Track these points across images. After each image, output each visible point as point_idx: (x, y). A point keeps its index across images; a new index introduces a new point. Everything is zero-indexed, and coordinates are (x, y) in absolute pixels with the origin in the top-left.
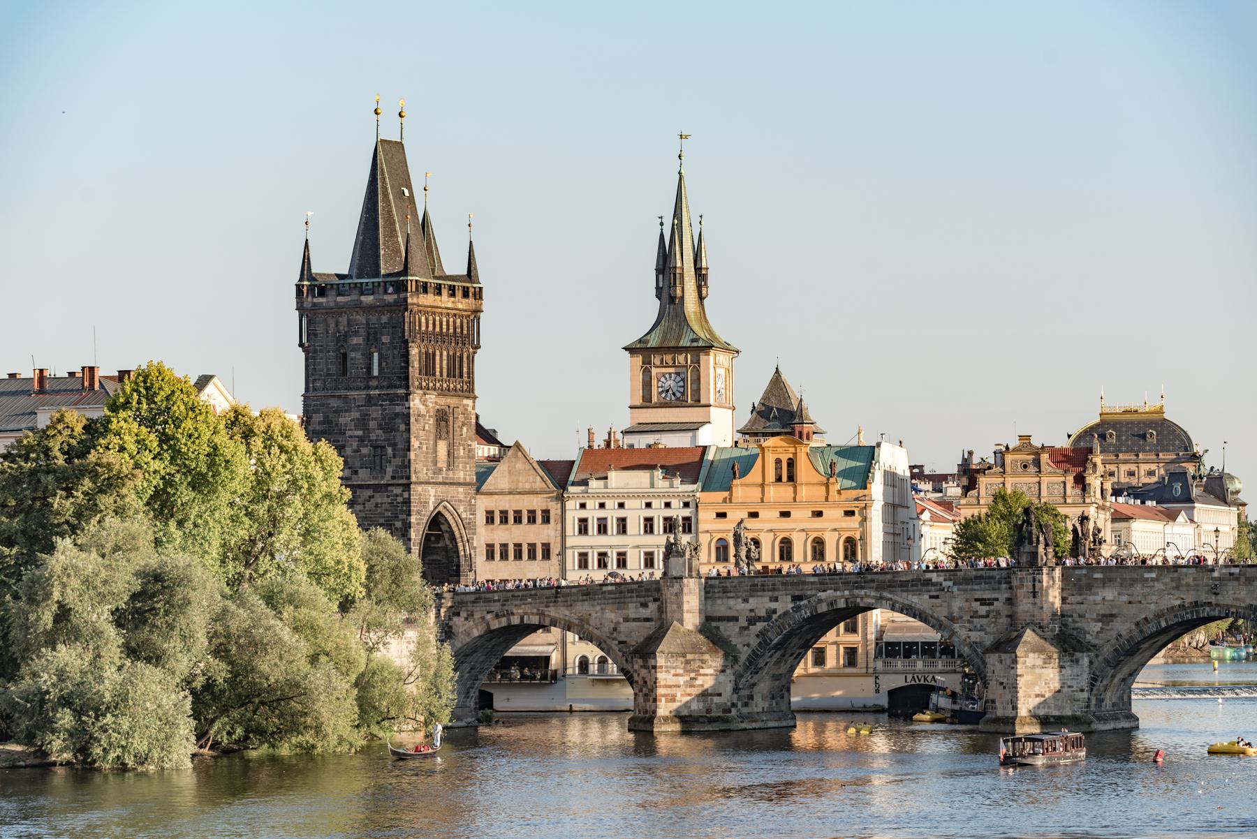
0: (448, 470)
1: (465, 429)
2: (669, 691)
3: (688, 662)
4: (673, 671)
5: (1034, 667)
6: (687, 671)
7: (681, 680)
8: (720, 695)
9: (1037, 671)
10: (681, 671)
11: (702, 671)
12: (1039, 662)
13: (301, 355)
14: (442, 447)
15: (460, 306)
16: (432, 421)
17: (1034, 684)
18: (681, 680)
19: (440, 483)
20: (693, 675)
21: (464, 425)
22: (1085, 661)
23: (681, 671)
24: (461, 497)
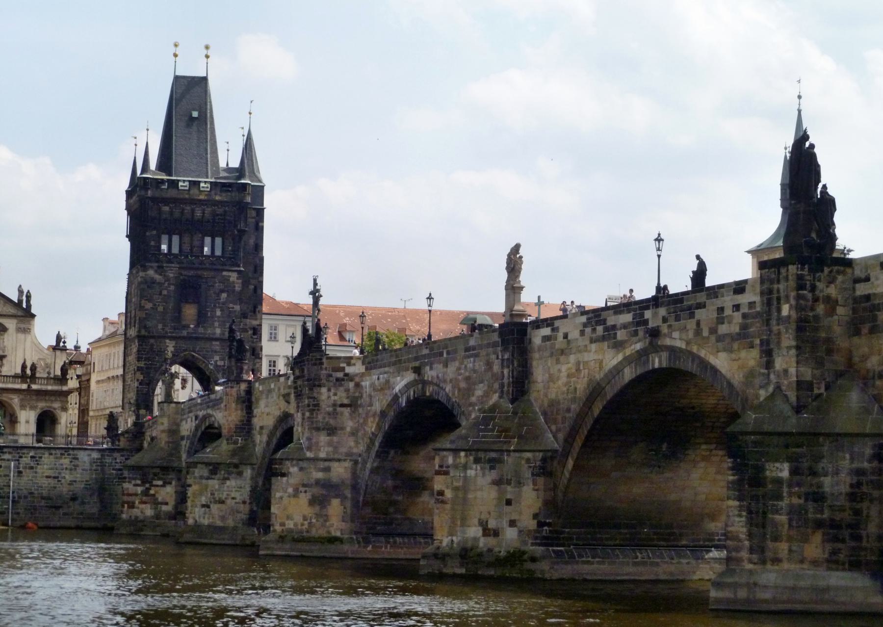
0: (198, 325)
1: (224, 295)
2: (130, 499)
3: (144, 475)
4: (133, 482)
5: (201, 477)
6: (144, 483)
7: (139, 490)
8: (167, 504)
9: (204, 481)
10: (139, 482)
11: (155, 483)
12: (205, 472)
13: (126, 245)
14: (190, 311)
15: (218, 198)
16: (172, 288)
17: (201, 494)
18: (139, 490)
19: (184, 338)
20: (147, 485)
21: (222, 291)
22: (248, 472)
23: (139, 482)
24: (218, 348)
